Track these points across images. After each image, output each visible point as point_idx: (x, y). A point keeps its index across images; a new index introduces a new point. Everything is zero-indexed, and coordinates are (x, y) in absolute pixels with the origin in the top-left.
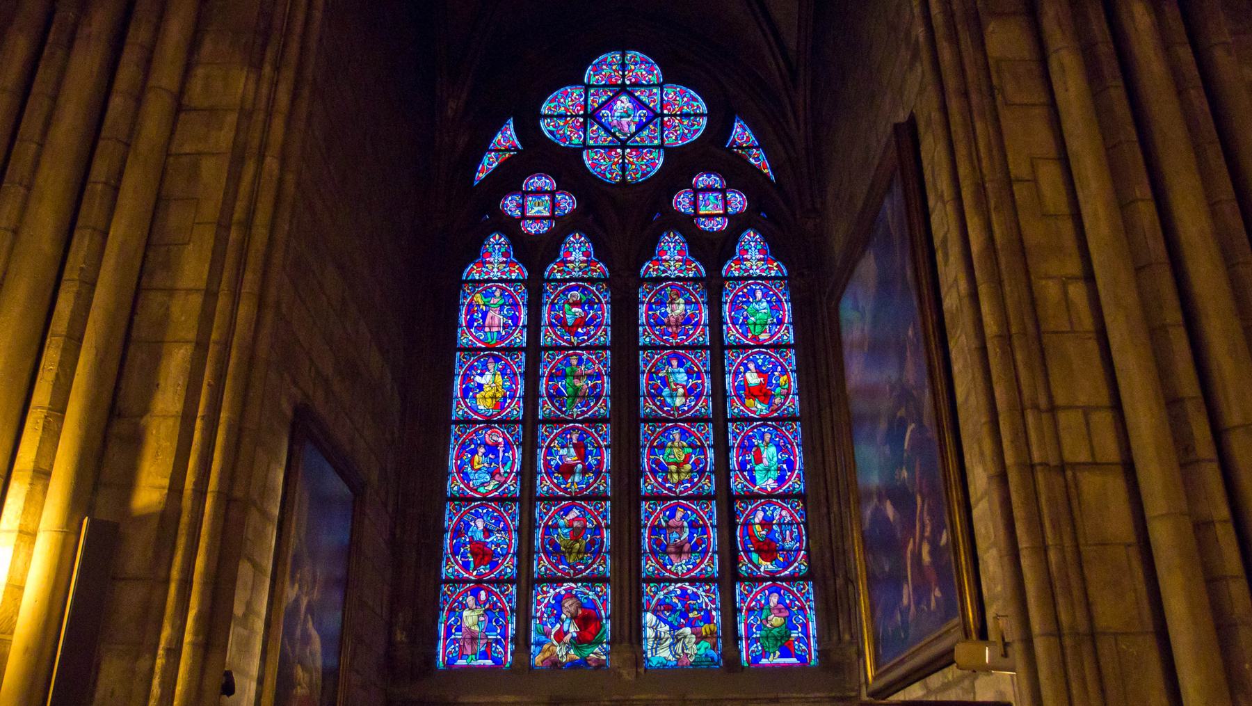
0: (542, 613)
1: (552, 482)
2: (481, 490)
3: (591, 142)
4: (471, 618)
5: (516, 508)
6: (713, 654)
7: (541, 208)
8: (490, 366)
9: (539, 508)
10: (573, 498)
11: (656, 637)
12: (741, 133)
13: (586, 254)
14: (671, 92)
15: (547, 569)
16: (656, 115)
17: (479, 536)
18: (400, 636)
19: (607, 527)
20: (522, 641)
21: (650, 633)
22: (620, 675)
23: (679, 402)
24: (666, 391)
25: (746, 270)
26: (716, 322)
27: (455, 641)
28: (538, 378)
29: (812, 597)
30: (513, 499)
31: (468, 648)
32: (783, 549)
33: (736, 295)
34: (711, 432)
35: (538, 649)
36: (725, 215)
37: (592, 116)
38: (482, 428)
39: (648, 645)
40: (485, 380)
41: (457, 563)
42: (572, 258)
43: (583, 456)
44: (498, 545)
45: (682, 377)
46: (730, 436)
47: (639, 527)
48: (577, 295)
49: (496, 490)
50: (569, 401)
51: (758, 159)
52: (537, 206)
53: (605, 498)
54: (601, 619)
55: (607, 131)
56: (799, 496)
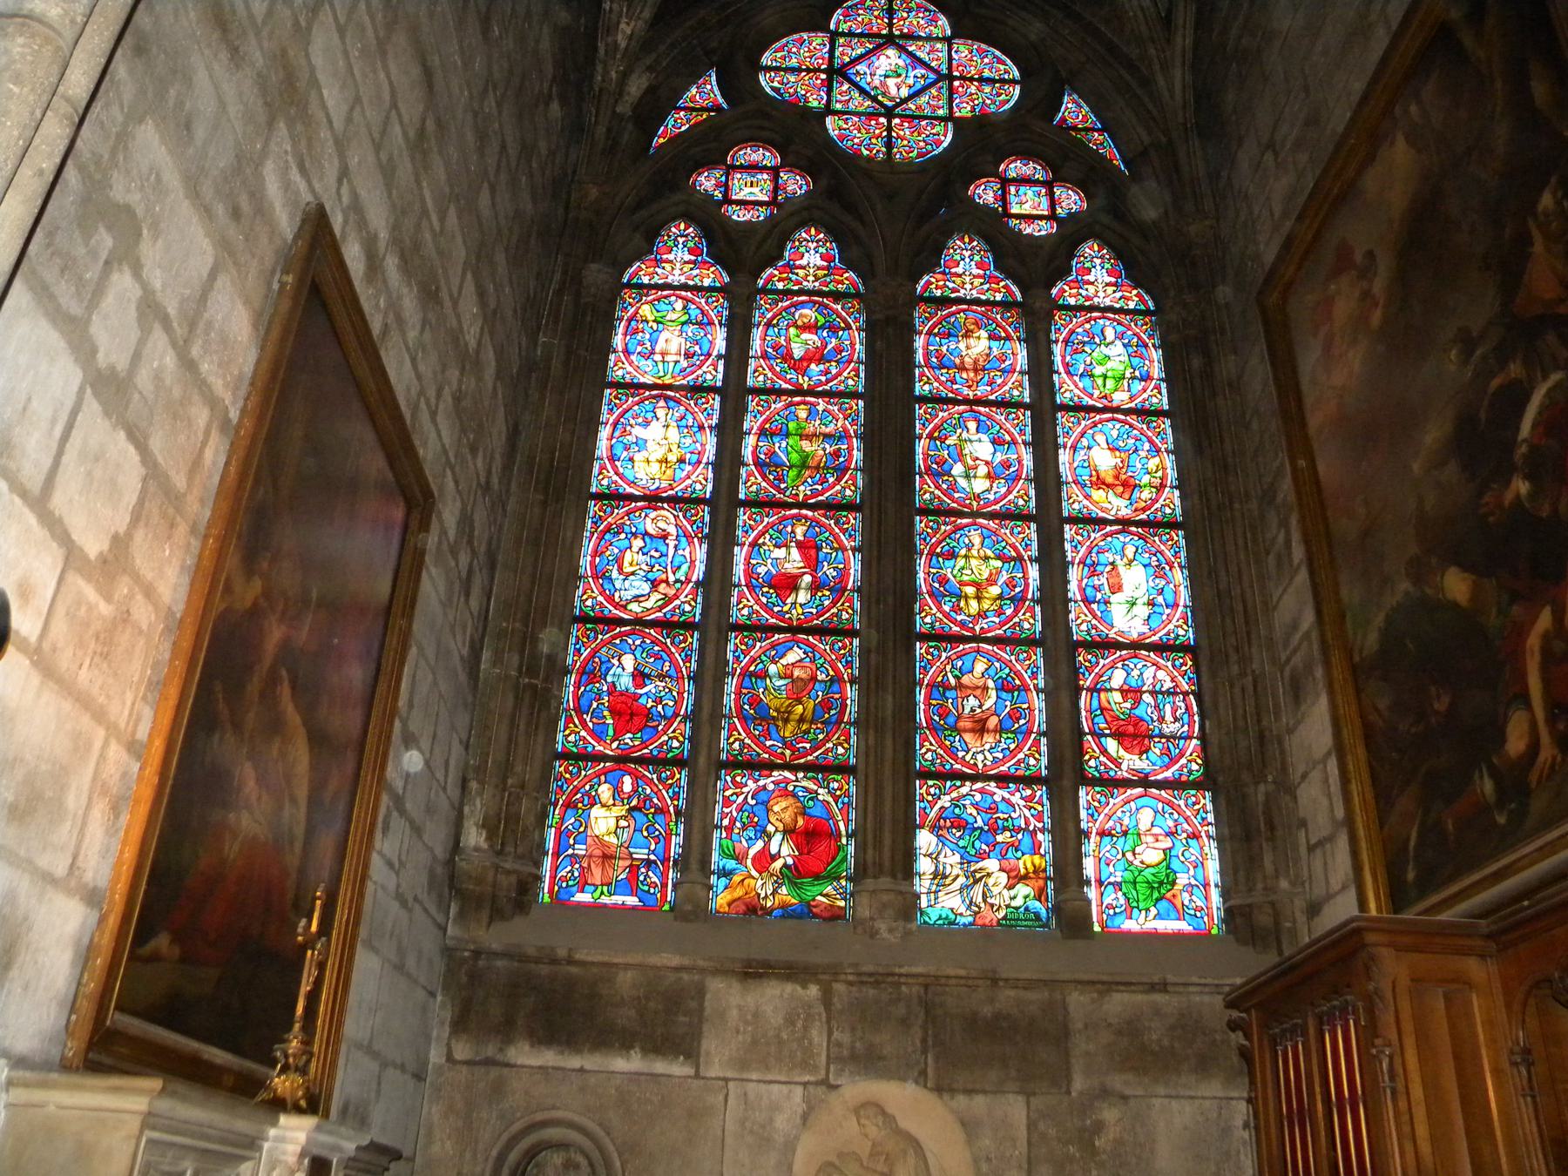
0: (733, 821)
1: (758, 601)
2: (634, 607)
3: (839, 107)
4: (604, 821)
5: (694, 640)
6: (1036, 905)
7: (756, 190)
8: (661, 413)
9: (734, 641)
10: (794, 630)
11: (935, 875)
12: (1072, 110)
13: (827, 258)
14: (962, 50)
15: (743, 745)
16: (940, 77)
17: (625, 682)
18: (474, 837)
19: (852, 682)
20: (695, 862)
21: (924, 865)
22: (873, 934)
23: (980, 485)
24: (958, 469)
25: (1088, 298)
26: (1041, 370)
27: (574, 858)
28: (741, 435)
29: (1211, 818)
30: (689, 626)
31: (597, 875)
32: (1161, 736)
33: (1072, 332)
34: (1034, 536)
35: (723, 881)
36: (1052, 216)
37: (837, 72)
38: (641, 509)
39: (922, 885)
40: (654, 432)
41: (584, 724)
42: (803, 262)
43: (812, 563)
44: (658, 701)
45: (982, 448)
46: (1067, 546)
47: (913, 684)
48: (808, 314)
49: (660, 608)
50: (793, 473)
51: (1102, 143)
52: (749, 187)
53: (851, 633)
54: (839, 835)
55: (862, 91)
56: (1184, 648)
